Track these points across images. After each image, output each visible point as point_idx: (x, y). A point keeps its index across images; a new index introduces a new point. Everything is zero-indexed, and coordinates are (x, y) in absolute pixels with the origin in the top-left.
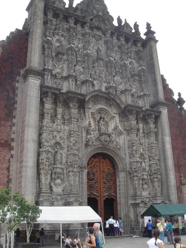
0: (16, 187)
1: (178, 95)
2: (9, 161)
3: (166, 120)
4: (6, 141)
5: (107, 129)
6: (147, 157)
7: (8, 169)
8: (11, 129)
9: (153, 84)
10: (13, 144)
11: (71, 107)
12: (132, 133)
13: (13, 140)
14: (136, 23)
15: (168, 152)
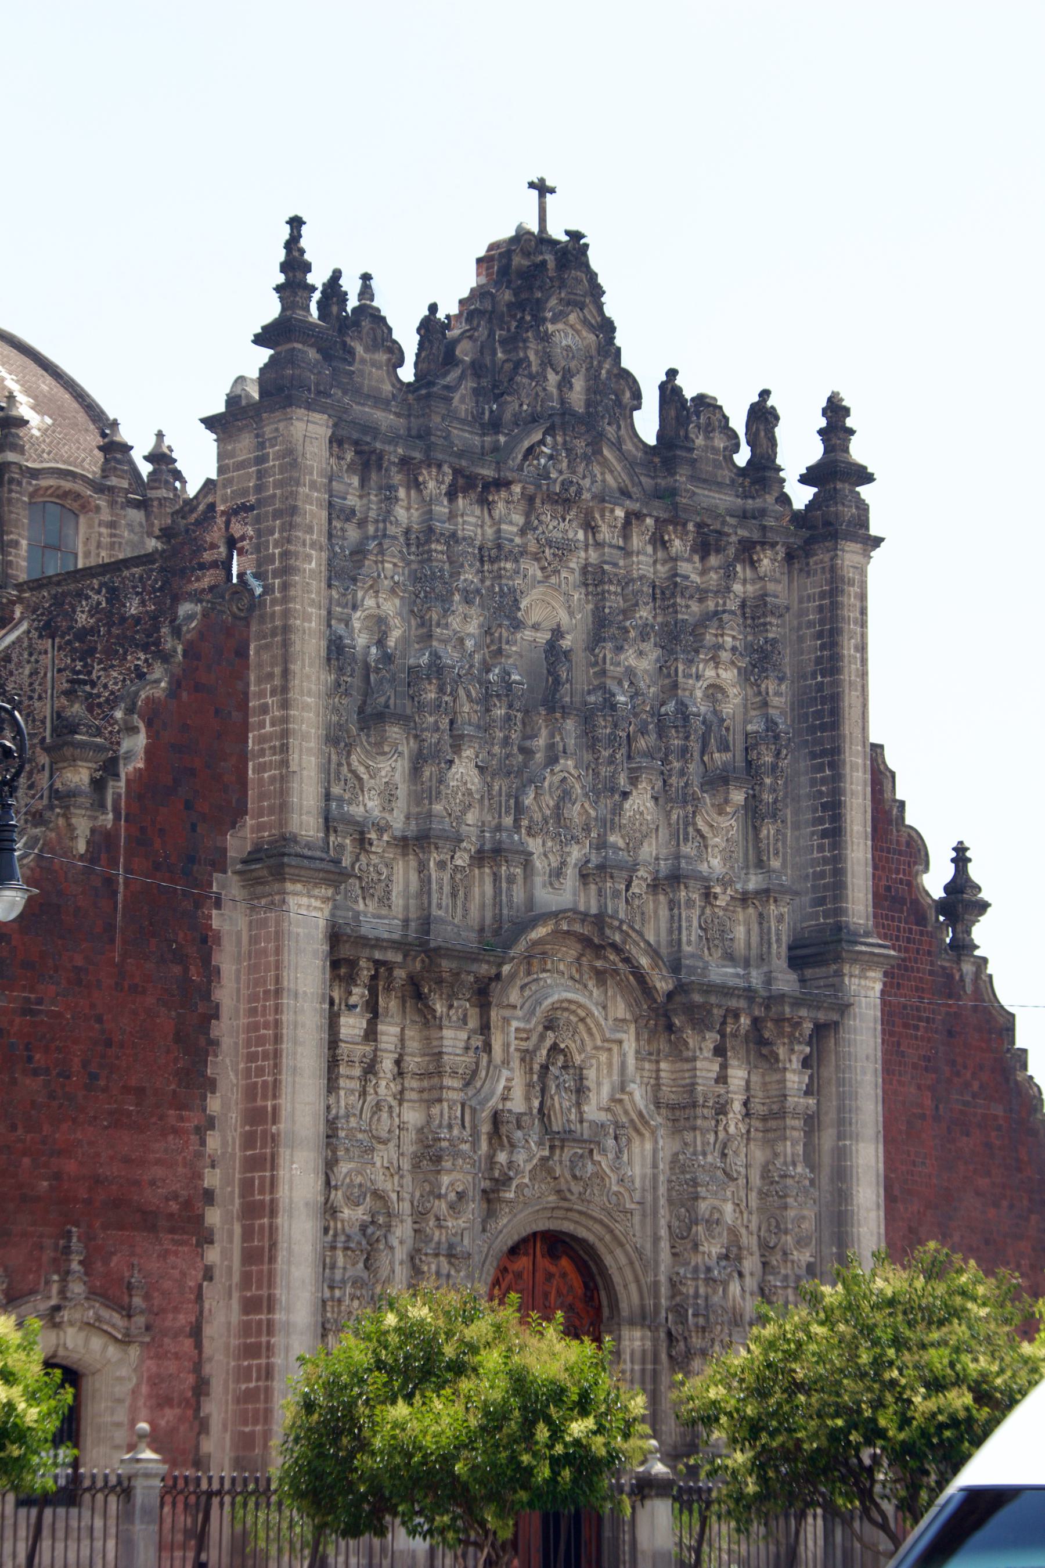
0: (226, 1412)
1: (953, 860)
2: (199, 1297)
3: (871, 1052)
4: (187, 1204)
5: (578, 1105)
6: (755, 1248)
7: (196, 1332)
8: (203, 1143)
9: (820, 821)
10: (213, 1217)
11: (438, 1014)
12: (694, 1129)
13: (209, 1196)
14: (765, 394)
15: (863, 1230)
